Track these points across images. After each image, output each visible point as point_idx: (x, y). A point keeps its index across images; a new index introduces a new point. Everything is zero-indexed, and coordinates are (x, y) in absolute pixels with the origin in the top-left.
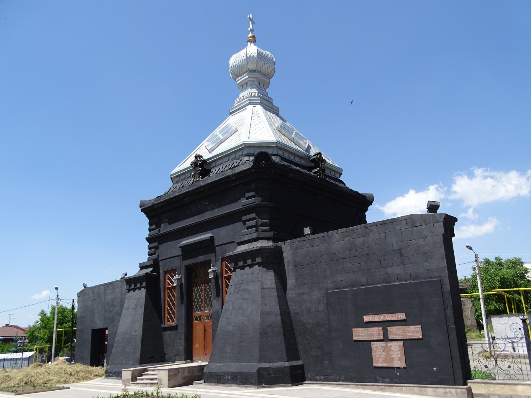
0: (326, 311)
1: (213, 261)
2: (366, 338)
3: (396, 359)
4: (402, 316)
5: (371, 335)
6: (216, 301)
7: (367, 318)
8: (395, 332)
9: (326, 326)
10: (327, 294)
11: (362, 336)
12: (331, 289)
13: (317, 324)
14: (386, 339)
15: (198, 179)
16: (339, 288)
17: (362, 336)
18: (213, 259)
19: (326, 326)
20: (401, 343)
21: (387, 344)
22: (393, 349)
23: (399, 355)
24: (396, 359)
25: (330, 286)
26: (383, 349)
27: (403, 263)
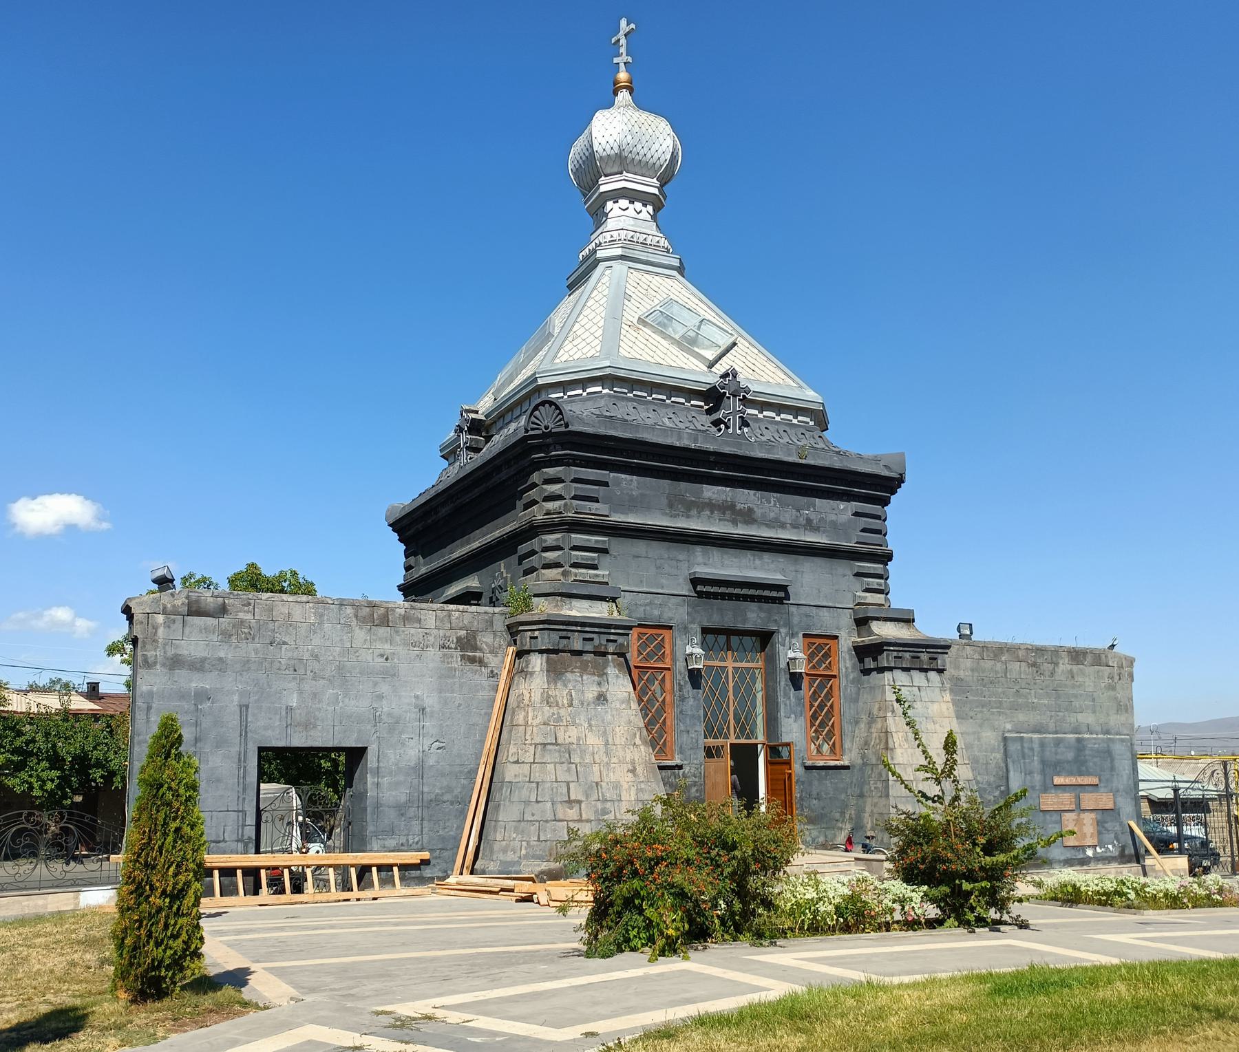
0: (1003, 765)
1: (783, 635)
2: (1056, 807)
3: (1089, 835)
4: (1095, 781)
5: (1062, 804)
6: (791, 720)
7: (1058, 780)
8: (1089, 800)
9: (1002, 788)
10: (1005, 739)
11: (1051, 805)
12: (1009, 731)
13: (989, 784)
14: (1080, 809)
15: (739, 432)
16: (1021, 733)
17: (1051, 805)
18: (783, 631)
19: (1002, 788)
20: (1093, 815)
21: (1079, 815)
22: (1085, 822)
23: (1091, 830)
24: (1089, 835)
25: (1009, 726)
26: (1075, 822)
27: (1094, 712)
